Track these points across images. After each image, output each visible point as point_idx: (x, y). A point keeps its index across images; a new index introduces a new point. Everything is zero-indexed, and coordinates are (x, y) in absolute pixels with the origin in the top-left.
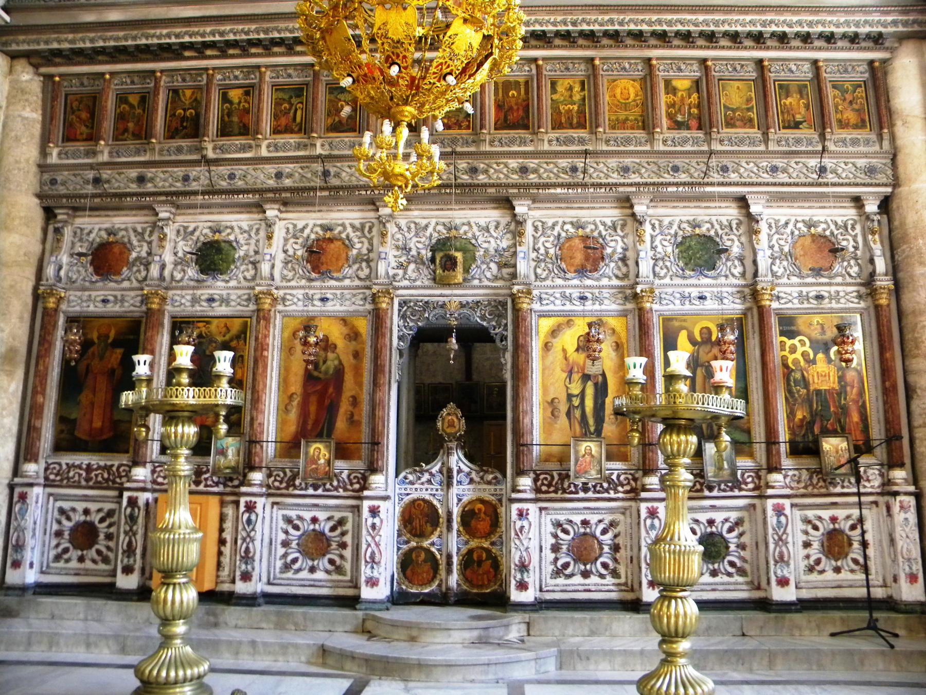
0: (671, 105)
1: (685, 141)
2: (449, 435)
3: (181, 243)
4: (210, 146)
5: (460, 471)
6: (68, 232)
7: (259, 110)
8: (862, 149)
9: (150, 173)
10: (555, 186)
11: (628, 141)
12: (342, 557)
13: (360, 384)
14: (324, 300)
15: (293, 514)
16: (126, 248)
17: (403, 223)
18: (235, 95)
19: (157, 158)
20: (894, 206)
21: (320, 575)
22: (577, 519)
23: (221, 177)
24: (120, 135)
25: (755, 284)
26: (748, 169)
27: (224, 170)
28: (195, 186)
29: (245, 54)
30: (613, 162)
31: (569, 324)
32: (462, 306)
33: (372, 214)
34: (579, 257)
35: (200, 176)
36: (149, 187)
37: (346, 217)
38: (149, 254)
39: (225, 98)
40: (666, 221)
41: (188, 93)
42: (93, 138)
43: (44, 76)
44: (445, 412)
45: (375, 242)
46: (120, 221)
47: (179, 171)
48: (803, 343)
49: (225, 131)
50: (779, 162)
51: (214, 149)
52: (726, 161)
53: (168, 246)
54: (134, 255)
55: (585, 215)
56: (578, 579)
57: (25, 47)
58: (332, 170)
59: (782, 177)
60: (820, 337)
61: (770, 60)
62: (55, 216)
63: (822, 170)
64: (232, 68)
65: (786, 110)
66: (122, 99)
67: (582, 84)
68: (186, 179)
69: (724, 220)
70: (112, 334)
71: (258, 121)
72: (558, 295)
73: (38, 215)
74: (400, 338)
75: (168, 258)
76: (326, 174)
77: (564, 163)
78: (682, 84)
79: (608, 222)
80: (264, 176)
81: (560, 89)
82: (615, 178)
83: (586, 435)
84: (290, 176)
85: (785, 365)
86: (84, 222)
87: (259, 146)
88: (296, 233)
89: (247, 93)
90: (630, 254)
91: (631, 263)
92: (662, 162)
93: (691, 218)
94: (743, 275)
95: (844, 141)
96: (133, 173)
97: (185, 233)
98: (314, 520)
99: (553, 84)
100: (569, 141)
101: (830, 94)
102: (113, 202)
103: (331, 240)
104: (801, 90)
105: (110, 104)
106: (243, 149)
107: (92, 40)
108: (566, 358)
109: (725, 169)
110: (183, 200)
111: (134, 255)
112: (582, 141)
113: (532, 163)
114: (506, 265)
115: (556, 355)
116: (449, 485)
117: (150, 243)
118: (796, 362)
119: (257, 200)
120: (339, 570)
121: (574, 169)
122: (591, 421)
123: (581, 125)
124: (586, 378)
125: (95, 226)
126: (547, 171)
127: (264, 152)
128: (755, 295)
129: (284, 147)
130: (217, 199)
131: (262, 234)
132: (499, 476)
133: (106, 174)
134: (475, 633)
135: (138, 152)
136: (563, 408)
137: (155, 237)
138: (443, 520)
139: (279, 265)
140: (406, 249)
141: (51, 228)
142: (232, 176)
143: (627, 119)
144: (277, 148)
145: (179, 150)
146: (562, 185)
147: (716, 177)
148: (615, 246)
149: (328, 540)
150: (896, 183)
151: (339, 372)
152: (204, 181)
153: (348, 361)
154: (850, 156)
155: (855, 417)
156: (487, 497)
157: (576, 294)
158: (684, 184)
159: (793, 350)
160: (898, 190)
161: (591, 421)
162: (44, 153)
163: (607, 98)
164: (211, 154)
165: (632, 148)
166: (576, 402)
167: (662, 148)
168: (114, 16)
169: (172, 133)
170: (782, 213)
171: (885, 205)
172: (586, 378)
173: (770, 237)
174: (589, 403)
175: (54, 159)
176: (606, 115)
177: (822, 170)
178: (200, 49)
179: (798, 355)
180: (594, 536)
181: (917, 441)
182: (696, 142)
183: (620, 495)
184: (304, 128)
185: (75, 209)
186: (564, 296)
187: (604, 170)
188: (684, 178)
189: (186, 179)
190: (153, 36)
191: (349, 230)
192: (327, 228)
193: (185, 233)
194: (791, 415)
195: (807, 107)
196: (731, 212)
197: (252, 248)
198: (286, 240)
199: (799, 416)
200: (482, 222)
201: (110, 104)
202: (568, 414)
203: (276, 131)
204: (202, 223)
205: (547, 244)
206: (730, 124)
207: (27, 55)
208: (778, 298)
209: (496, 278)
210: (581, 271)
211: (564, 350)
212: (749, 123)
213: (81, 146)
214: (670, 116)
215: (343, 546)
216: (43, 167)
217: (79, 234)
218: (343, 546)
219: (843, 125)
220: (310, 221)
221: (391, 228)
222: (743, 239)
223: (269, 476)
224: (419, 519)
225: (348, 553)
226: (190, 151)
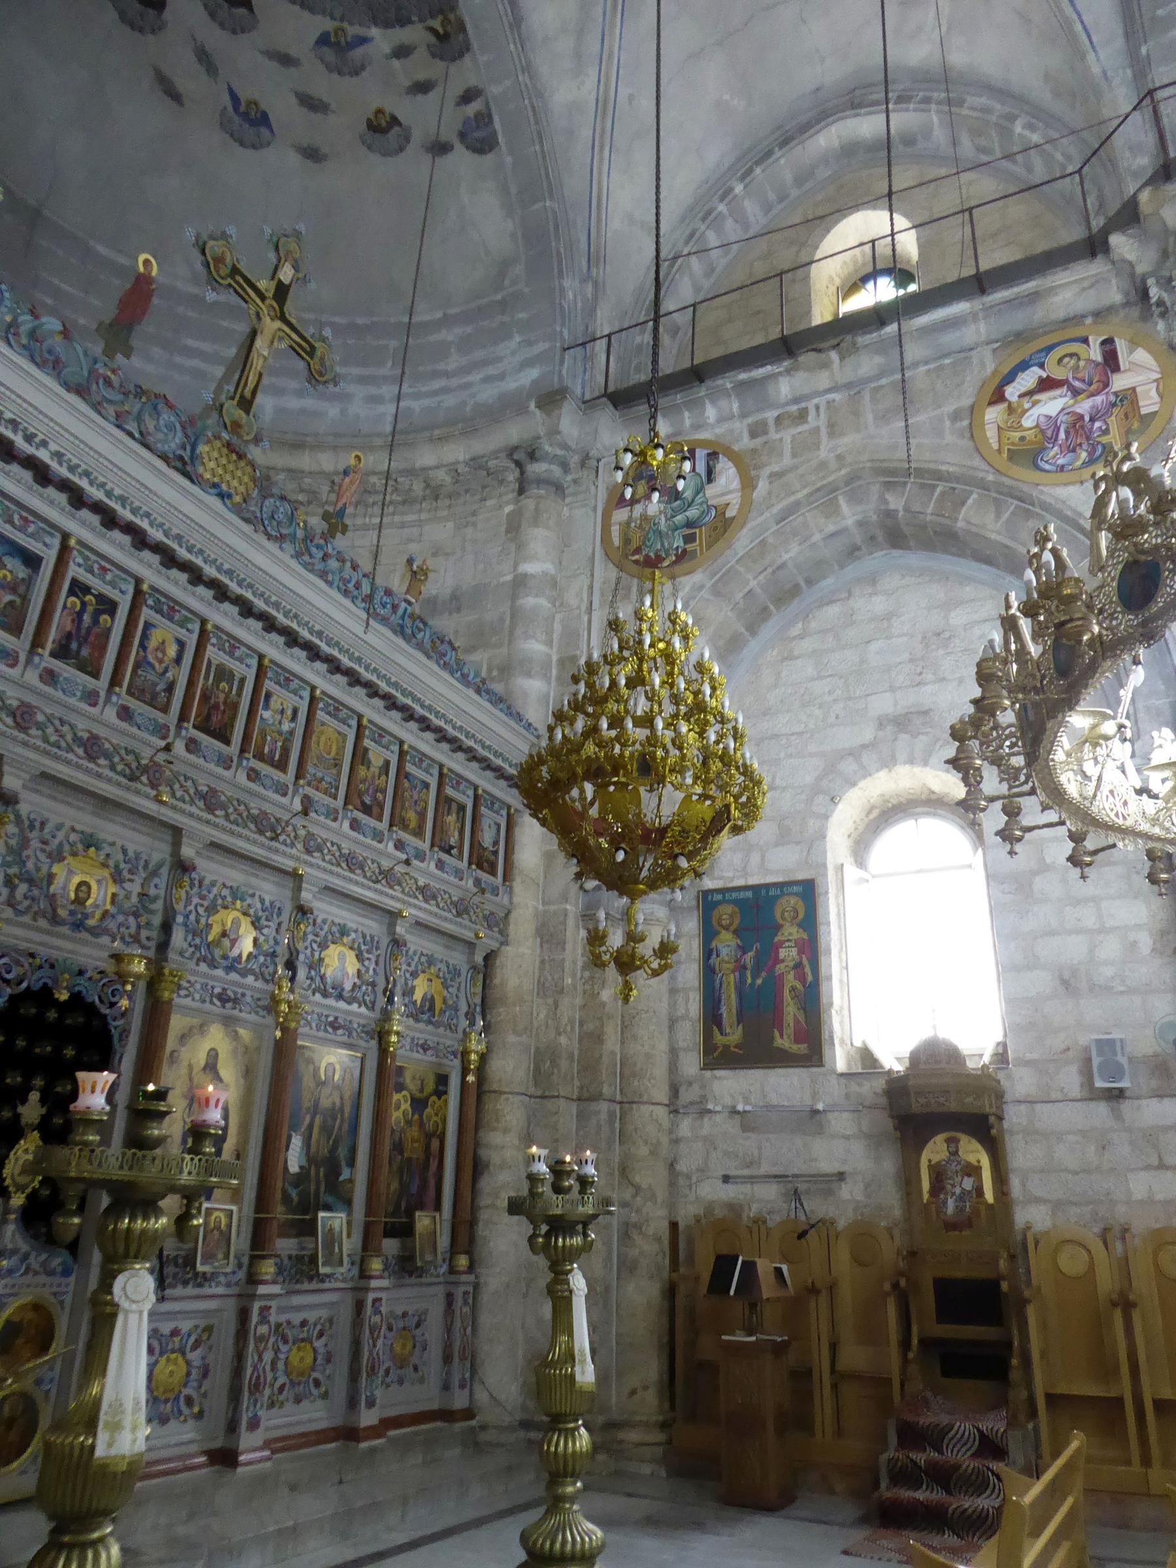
2: (16, 1185)
20: (498, 962)
60: (418, 1095)
72: (198, 986)
93: (342, 922)
108: (191, 1079)
132: (70, 1259)
143: (322, 779)
181: (481, 1225)
183: (220, 1290)
211: (190, 1067)
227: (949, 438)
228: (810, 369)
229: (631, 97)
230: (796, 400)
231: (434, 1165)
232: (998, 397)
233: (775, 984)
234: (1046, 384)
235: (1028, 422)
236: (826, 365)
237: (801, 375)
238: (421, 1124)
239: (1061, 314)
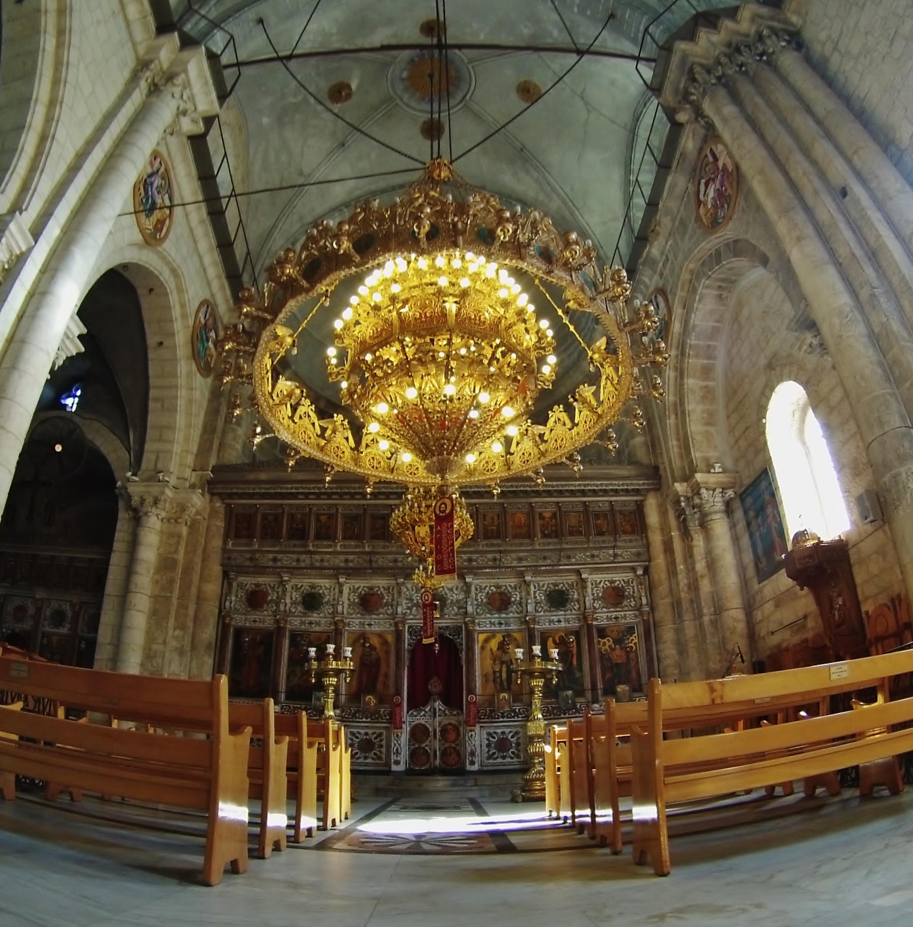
0: (542, 526)
1: (549, 544)
3: (294, 594)
4: (311, 545)
5: (440, 710)
6: (235, 585)
7: (336, 527)
8: (634, 544)
9: (279, 556)
10: (486, 568)
11: (521, 545)
12: (381, 752)
13: (388, 667)
14: (370, 625)
15: (355, 731)
16: (266, 594)
17: (409, 586)
18: (323, 518)
19: (283, 549)
21: (369, 761)
22: (499, 731)
23: (317, 561)
24: (263, 537)
25: (585, 612)
26: (580, 556)
27: (318, 557)
28: (303, 565)
29: (330, 498)
30: (514, 555)
31: (494, 636)
32: (440, 628)
33: (393, 582)
34: (498, 603)
35: (306, 560)
36: (279, 564)
37: (380, 583)
38: (278, 598)
39: (318, 520)
40: (541, 584)
41: (299, 516)
42: (250, 537)
43: (226, 504)
44: (432, 681)
45: (395, 596)
46: (261, 580)
47: (294, 556)
48: (609, 641)
49: (318, 537)
50: (596, 553)
51: (313, 546)
52: (569, 553)
53: (288, 595)
54: (269, 598)
55: (501, 582)
56: (500, 760)
57: (221, 491)
58: (374, 559)
59: (597, 560)
61: (589, 502)
62: (228, 575)
63: (615, 555)
64: (322, 505)
65: (597, 526)
66: (265, 517)
67: (498, 516)
68: (298, 560)
69: (570, 582)
70: (258, 638)
71: (336, 532)
73: (220, 574)
74: (409, 645)
75: (288, 601)
76: (371, 561)
77: (490, 556)
78: (547, 515)
79: (512, 585)
80: (339, 561)
81: (488, 518)
82: (515, 564)
83: (503, 690)
84: (352, 561)
85: (601, 652)
86: (241, 579)
87: (336, 546)
88: (354, 590)
89: (329, 518)
90: (524, 601)
91: (524, 605)
92: (538, 554)
94: (579, 609)
95: (625, 541)
96: (271, 556)
97: (296, 588)
98: (366, 734)
99: (484, 516)
100: (493, 545)
101: (618, 516)
102: (261, 570)
103: (372, 594)
104: (605, 516)
105: (259, 519)
106: (330, 546)
107: (253, 489)
109: (569, 557)
110: (296, 572)
111: (269, 598)
112: (499, 545)
113: (474, 556)
114: (461, 608)
115: (487, 652)
116: (435, 716)
117: (278, 592)
118: (606, 650)
119: (336, 572)
120: (380, 758)
121: (495, 559)
122: (505, 684)
123: (498, 537)
124: (502, 663)
125: (249, 581)
126: (481, 560)
127: (339, 549)
128: (585, 618)
129: (349, 546)
130: (314, 572)
131: (337, 590)
133: (257, 555)
134: (450, 782)
135: (273, 546)
136: (491, 678)
137: (280, 590)
138: (432, 734)
139: (346, 606)
140: (411, 600)
141: (226, 582)
142: (322, 561)
144: (345, 547)
145: (295, 546)
146: (489, 568)
147: (564, 561)
148: (516, 597)
149: (374, 744)
150: (650, 560)
151: (378, 660)
152: (308, 563)
153: (382, 655)
154: (627, 549)
155: (634, 674)
156: (454, 722)
157: (497, 621)
158: (549, 566)
159: (604, 644)
160: (652, 563)
161: (505, 684)
162: (225, 543)
163: (511, 523)
164: (311, 548)
165: (523, 548)
166: (498, 675)
167: (537, 547)
168: (263, 476)
169: (291, 537)
170: (597, 577)
171: (646, 570)
172: (502, 663)
173: (592, 589)
174: (504, 675)
175: (230, 546)
176: (510, 530)
177: (615, 555)
178: (307, 496)
179: (607, 647)
180: (507, 739)
182: (555, 544)
184: (359, 538)
185: (238, 572)
186: (491, 623)
187: (510, 560)
188: (549, 562)
189: (298, 560)
190: (284, 488)
191: (382, 589)
192: (371, 588)
193: (296, 588)
194: (603, 676)
195: (608, 524)
196: (573, 578)
197: (332, 597)
198: (349, 594)
199: (608, 676)
200: (450, 586)
201: (259, 519)
202: (494, 681)
203: (344, 538)
204: (305, 583)
205: (482, 597)
206: (571, 534)
207: (219, 495)
208: (597, 619)
209: (456, 614)
210: (499, 610)
211: (491, 650)
212: (580, 533)
213: (244, 541)
214: (542, 532)
215: (381, 746)
216: (224, 550)
217: (241, 586)
218: (381, 746)
219: (625, 532)
220: (362, 584)
221: (404, 589)
222: (580, 591)
223: (343, 712)
224: (419, 733)
225: (384, 750)
226: (301, 546)
227: (698, 232)
228: (656, 240)
229: (572, 189)
230: (662, 254)
231: (633, 663)
232: (699, 202)
233: (769, 527)
234: (707, 185)
235: (709, 206)
236: (658, 234)
237: (656, 244)
238: (622, 649)
239: (696, 153)
